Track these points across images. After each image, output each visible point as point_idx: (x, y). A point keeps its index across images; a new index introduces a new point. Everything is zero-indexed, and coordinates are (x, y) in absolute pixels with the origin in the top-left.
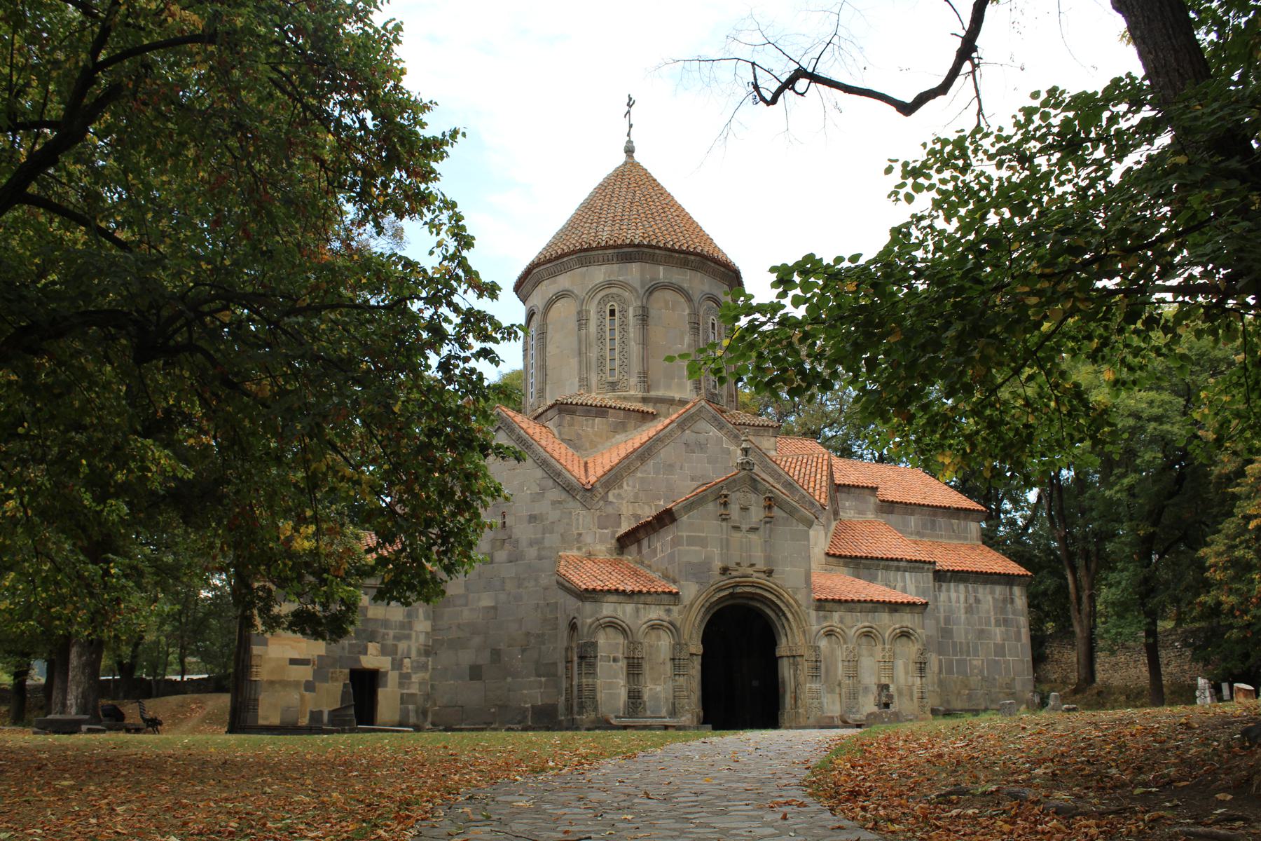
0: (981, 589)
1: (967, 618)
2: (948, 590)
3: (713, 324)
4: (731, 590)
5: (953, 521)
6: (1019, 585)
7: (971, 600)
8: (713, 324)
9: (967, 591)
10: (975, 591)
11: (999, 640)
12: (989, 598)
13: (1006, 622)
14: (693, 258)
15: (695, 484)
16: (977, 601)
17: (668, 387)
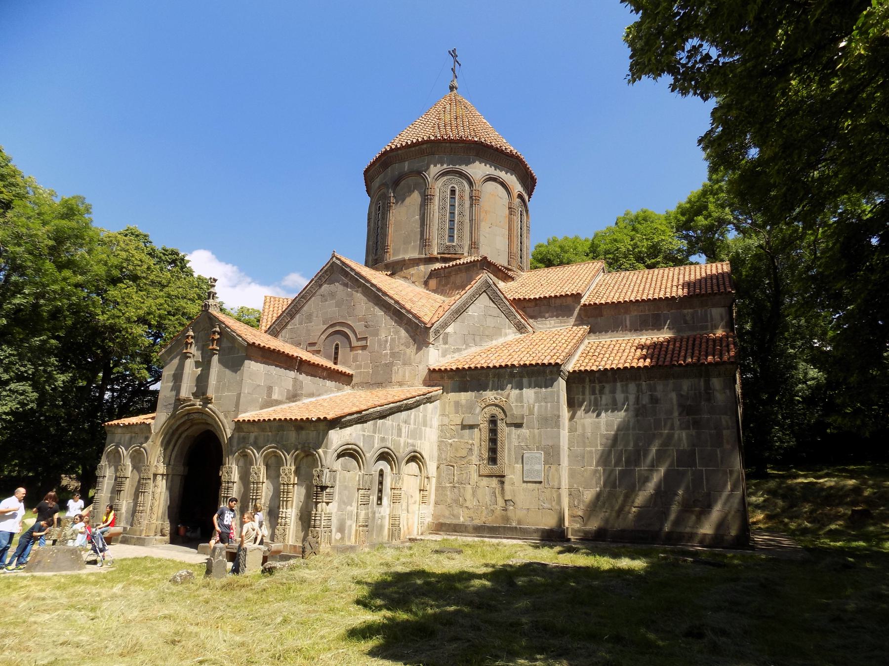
0: (660, 387)
1: (638, 421)
2: (613, 391)
3: (453, 192)
4: (186, 417)
5: (685, 311)
6: (719, 375)
7: (645, 400)
8: (453, 192)
9: (639, 389)
10: (652, 389)
11: (685, 445)
12: (674, 396)
13: (697, 424)
14: (425, 146)
15: (325, 327)
16: (654, 400)
17: (406, 252)
